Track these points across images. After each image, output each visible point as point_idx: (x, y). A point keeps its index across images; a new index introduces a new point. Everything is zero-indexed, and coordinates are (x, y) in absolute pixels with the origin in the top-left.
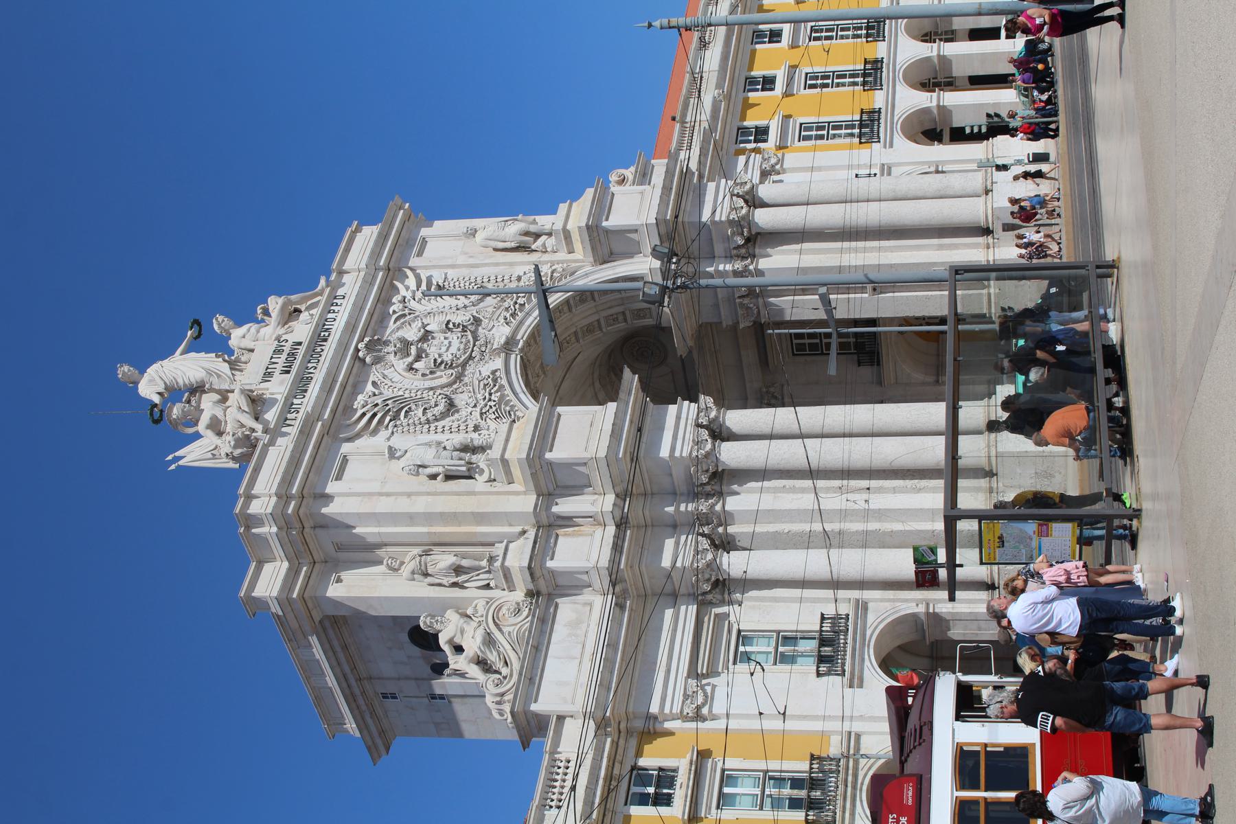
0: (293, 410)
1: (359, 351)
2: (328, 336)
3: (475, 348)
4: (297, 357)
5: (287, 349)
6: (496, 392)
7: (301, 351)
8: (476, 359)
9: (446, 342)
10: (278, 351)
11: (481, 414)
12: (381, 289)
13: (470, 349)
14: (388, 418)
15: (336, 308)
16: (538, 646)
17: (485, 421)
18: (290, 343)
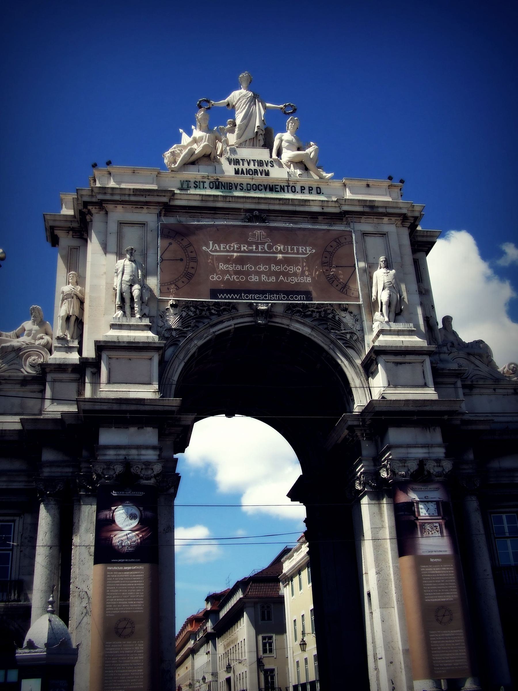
5: (265, 168)
7: (260, 179)
10: (260, 163)
17: (182, 311)
18: (269, 168)
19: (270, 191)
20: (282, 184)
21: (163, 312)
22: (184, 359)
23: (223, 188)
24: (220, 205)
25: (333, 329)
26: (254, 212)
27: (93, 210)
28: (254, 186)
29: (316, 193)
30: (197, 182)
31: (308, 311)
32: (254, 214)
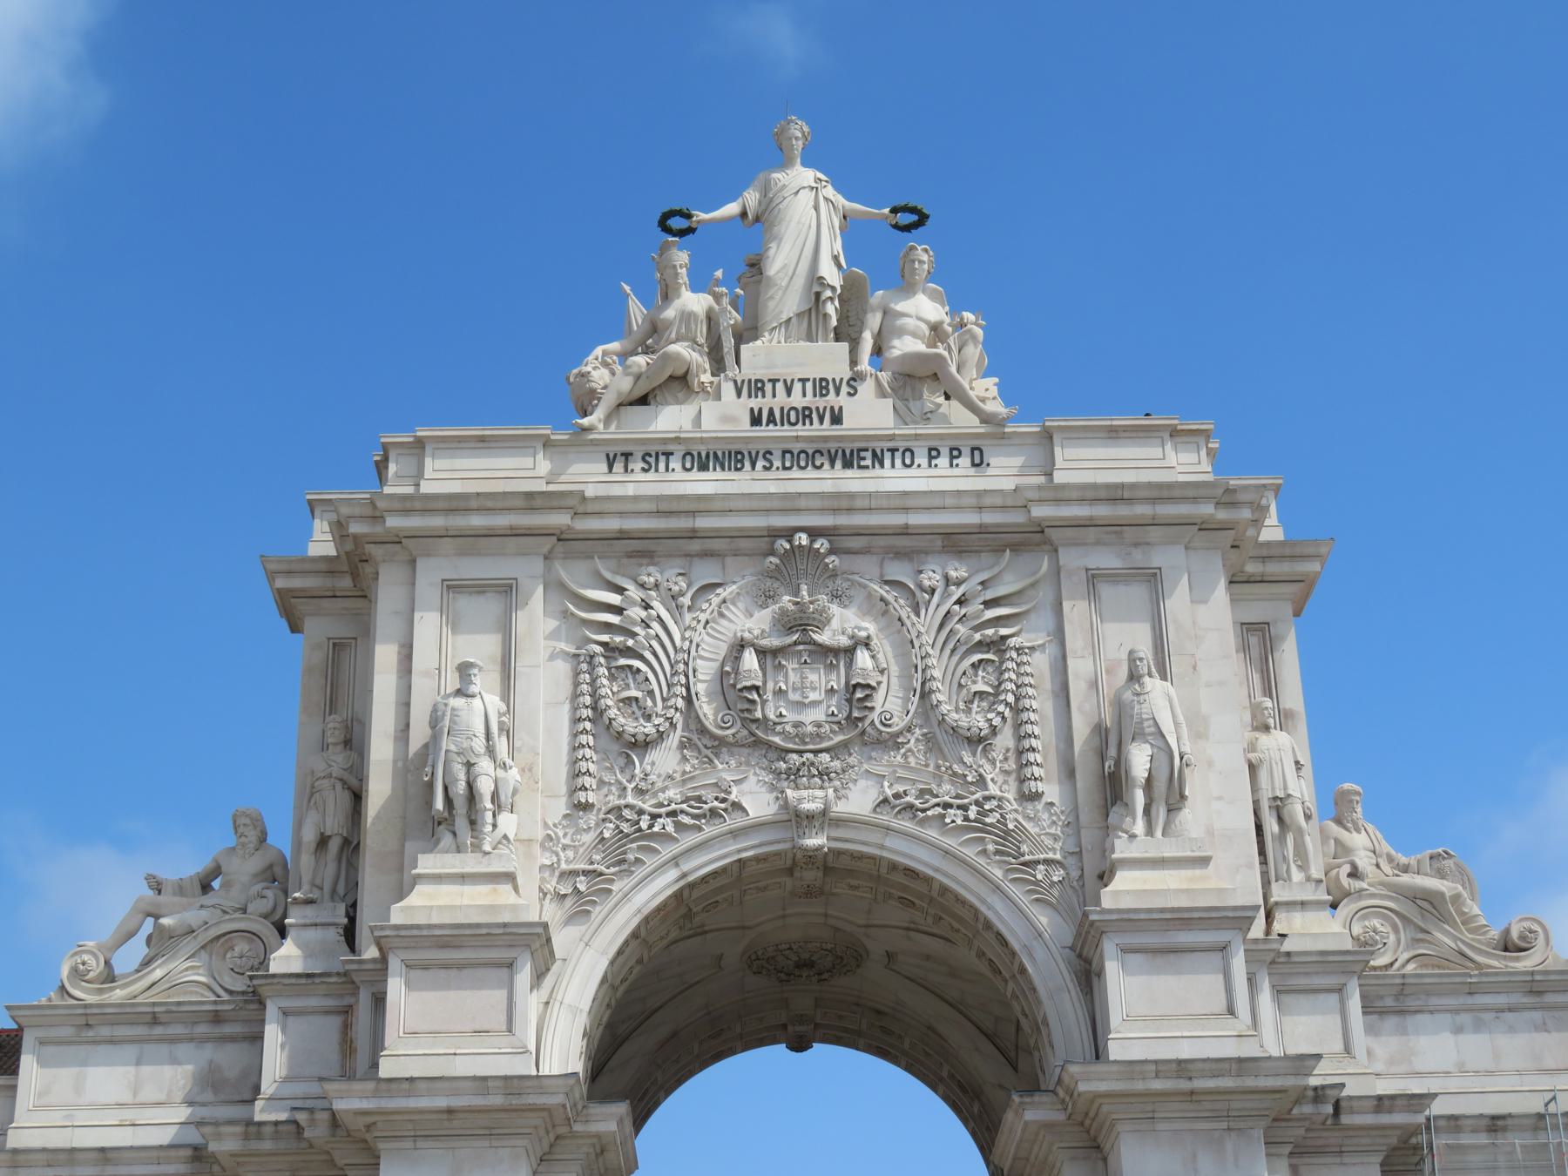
0: (652, 460)
1: (790, 542)
2: (860, 467)
3: (812, 755)
4: (800, 426)
6: (679, 826)
8: (783, 765)
9: (813, 696)
10: (822, 386)
11: (619, 808)
12: (982, 530)
13: (802, 748)
14: (605, 638)
15: (943, 461)
16: (160, 1023)
18: (843, 400)
19: (844, 467)
20: (878, 446)
21: (555, 825)
22: (604, 953)
23: (718, 469)
24: (703, 523)
25: (997, 852)
26: (797, 536)
27: (376, 551)
28: (803, 456)
29: (969, 465)
30: (650, 456)
31: (933, 807)
32: (797, 543)
